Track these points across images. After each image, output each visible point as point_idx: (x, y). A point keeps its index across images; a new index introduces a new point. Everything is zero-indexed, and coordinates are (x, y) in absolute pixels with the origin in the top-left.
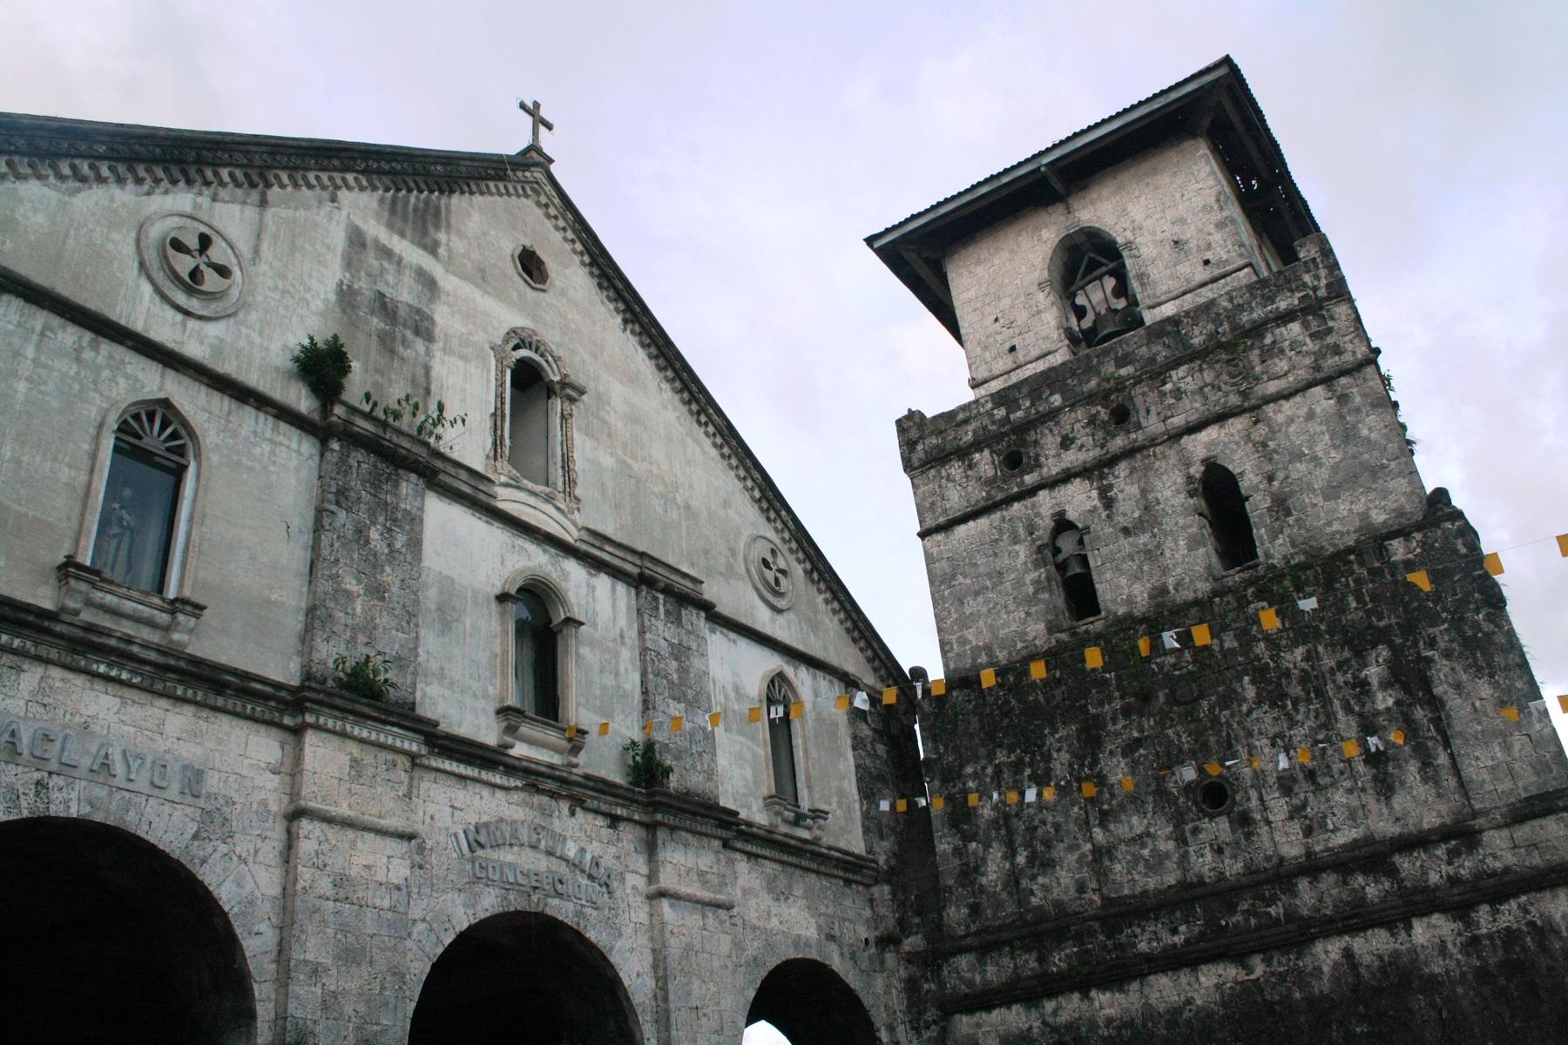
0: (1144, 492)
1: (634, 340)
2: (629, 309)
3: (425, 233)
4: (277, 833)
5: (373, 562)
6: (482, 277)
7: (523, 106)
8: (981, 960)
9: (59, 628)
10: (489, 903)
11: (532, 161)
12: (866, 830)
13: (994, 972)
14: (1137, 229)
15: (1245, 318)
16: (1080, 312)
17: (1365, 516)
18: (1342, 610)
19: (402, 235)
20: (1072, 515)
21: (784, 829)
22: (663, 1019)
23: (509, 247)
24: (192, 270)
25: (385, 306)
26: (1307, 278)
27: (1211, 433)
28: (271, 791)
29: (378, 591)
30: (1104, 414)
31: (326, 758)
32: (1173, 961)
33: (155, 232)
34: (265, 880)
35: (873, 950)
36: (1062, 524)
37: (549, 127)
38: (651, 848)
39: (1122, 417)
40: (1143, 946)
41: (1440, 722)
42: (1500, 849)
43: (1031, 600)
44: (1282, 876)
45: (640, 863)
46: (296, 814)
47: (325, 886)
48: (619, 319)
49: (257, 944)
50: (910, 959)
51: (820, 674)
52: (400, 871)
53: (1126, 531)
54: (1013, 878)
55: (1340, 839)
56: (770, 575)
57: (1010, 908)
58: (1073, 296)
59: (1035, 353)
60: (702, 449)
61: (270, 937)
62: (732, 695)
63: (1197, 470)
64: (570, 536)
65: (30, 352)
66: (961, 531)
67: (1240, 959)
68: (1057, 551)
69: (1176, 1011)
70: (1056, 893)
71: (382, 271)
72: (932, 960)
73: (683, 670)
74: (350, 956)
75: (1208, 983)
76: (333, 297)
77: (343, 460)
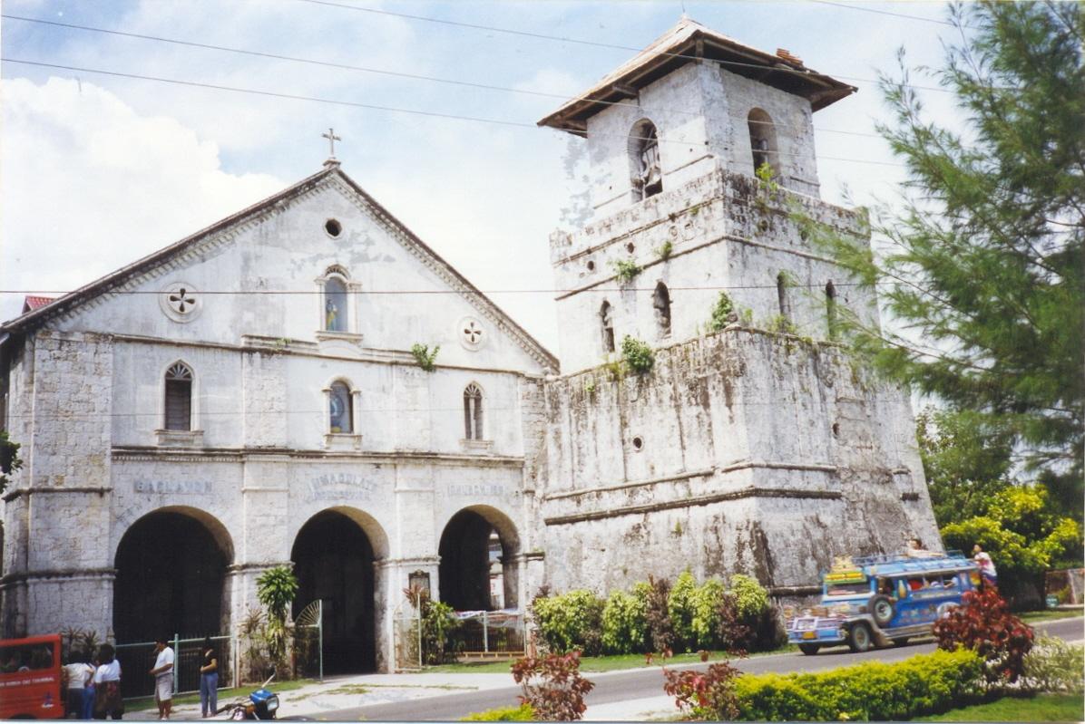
9: (159, 452)
16: (645, 165)
56: (469, 337)
58: (642, 155)
63: (655, 285)
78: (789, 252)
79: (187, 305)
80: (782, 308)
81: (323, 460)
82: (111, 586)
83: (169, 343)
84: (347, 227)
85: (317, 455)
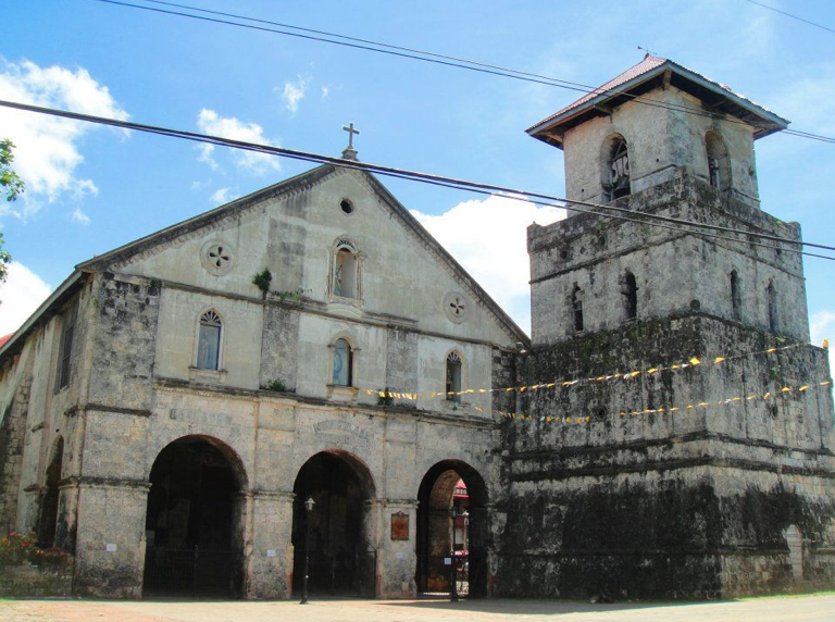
0: (605, 279)
1: (395, 221)
2: (393, 208)
3: (300, 210)
4: (253, 432)
5: (282, 346)
6: (325, 220)
7: (345, 129)
8: (524, 462)
10: (321, 448)
11: (349, 153)
12: (493, 408)
13: (527, 468)
14: (635, 137)
15: (651, 203)
17: (673, 305)
18: (652, 347)
19: (291, 215)
20: (579, 285)
21: (451, 412)
22: (384, 481)
23: (337, 201)
24: (218, 257)
25: (285, 248)
26: (675, 187)
27: (630, 256)
28: (251, 421)
29: (283, 354)
30: (596, 241)
31: (269, 407)
32: (578, 473)
33: (205, 251)
34: (251, 446)
35: (489, 455)
36: (577, 288)
37: (358, 133)
38: (385, 424)
39: (602, 242)
40: (570, 466)
41: (671, 399)
42: (678, 450)
43: (562, 319)
44: (613, 448)
45: (381, 431)
46: (258, 427)
47: (266, 447)
48: (388, 214)
49: (248, 464)
50: (504, 458)
51: (478, 346)
52: (290, 441)
53: (596, 295)
54: (538, 434)
55: (634, 438)
56: (455, 310)
57: (535, 445)
59: (591, 194)
60: (430, 257)
61: (252, 461)
62: (429, 362)
63: (623, 273)
64: (356, 313)
65: (174, 304)
66: (544, 283)
67: (597, 476)
68: (574, 298)
69: (575, 492)
70: (549, 442)
71: (284, 233)
72: (509, 460)
73: (405, 359)
74: (274, 466)
75: (584, 484)
76: (266, 252)
77: (270, 312)
78: (742, 253)
79: (223, 261)
80: (733, 301)
81: (325, 408)
82: (146, 497)
83: (206, 292)
84: (355, 202)
85: (319, 402)
